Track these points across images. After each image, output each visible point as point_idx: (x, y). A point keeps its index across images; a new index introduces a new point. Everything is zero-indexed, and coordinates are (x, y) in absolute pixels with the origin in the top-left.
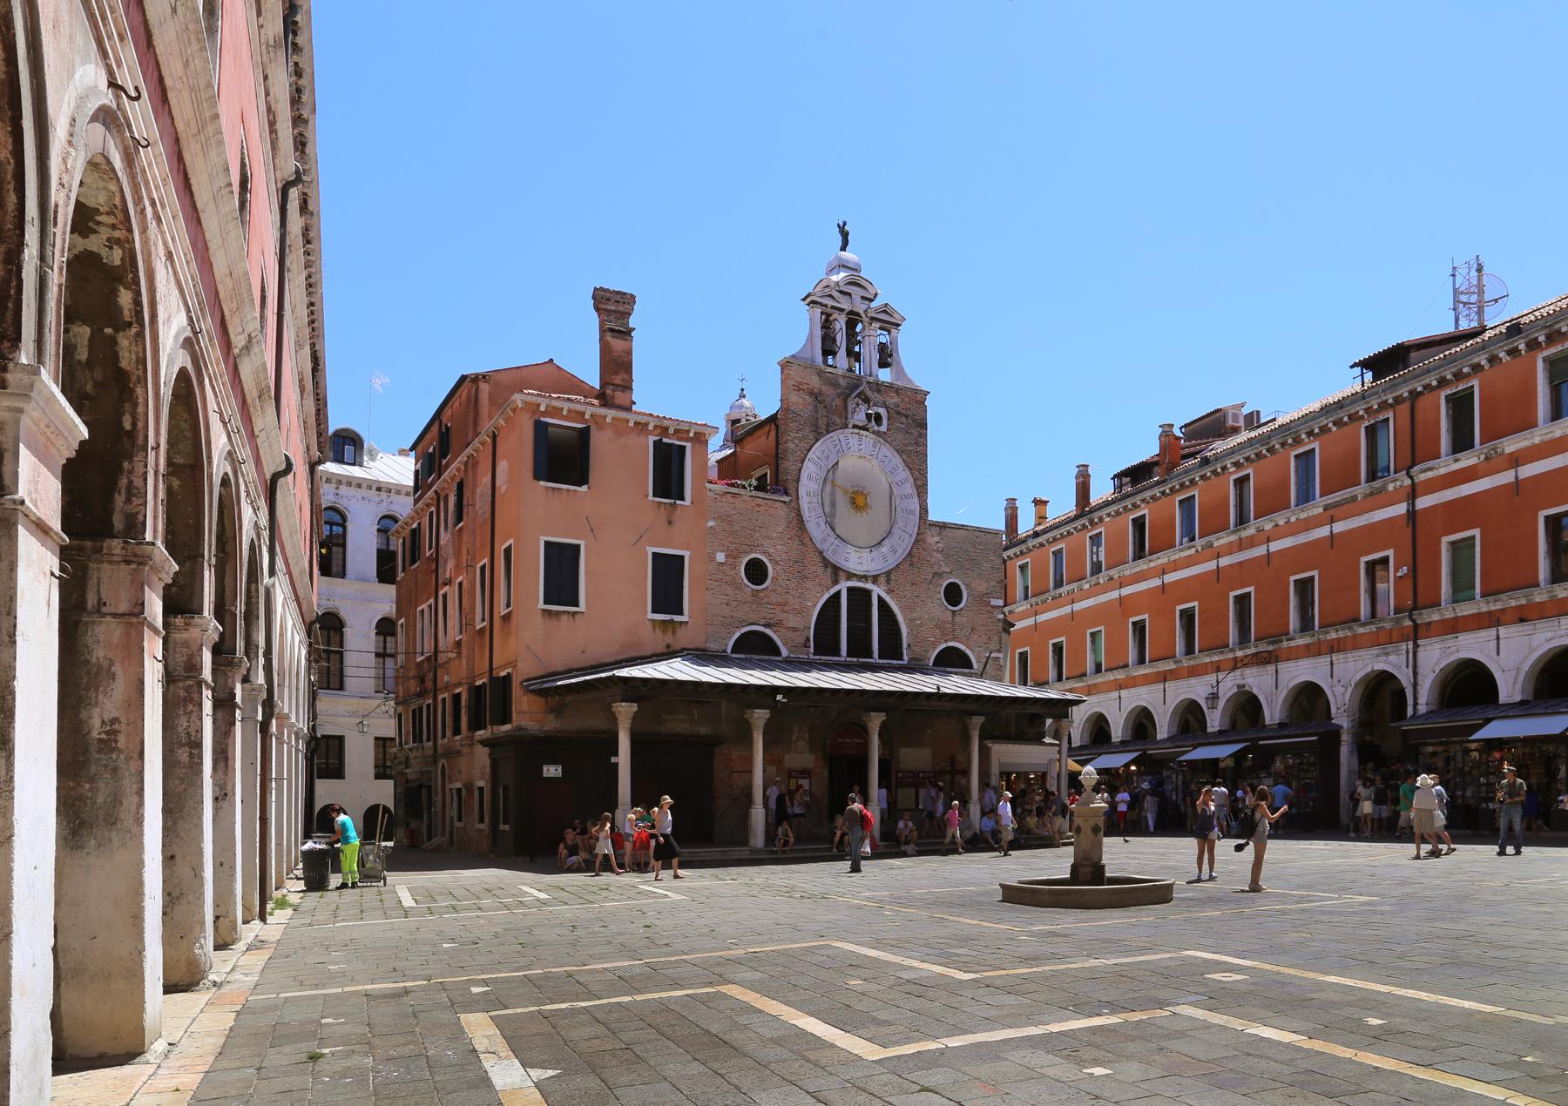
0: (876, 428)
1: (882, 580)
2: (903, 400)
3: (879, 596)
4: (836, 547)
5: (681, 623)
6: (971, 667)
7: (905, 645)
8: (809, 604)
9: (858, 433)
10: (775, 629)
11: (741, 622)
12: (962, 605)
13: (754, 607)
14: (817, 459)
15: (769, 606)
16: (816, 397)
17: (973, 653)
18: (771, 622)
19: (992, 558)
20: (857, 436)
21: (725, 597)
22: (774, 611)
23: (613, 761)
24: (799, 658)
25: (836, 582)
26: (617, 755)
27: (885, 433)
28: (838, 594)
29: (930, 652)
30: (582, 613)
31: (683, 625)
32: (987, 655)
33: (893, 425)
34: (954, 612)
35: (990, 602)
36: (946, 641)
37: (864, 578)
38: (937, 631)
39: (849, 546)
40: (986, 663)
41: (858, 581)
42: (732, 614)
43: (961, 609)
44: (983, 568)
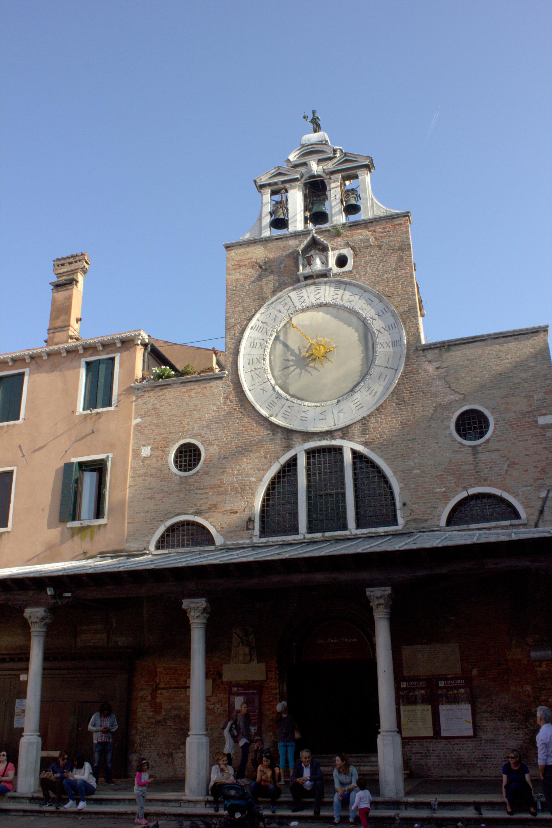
0: (336, 269)
1: (356, 430)
2: (374, 231)
3: (355, 453)
4: (289, 410)
5: (100, 526)
6: (517, 516)
7: (398, 505)
8: (253, 479)
9: (314, 284)
10: (207, 515)
11: (166, 515)
12: (487, 436)
13: (182, 496)
14: (261, 325)
15: (200, 491)
16: (260, 267)
17: (516, 496)
18: (203, 508)
19: (532, 364)
20: (313, 288)
21: (149, 491)
22: (204, 496)
23: (21, 679)
24: (238, 544)
25: (288, 448)
26: (27, 673)
27: (351, 272)
28: (294, 459)
29: (440, 508)
30: (8, 532)
31: (102, 528)
32: (543, 494)
33: (361, 261)
34: (474, 447)
35: (537, 421)
36: (465, 489)
37: (329, 434)
38: (449, 478)
39: (306, 403)
40: (543, 507)
41: (320, 440)
42: (156, 507)
43: (487, 441)
44: (516, 381)
